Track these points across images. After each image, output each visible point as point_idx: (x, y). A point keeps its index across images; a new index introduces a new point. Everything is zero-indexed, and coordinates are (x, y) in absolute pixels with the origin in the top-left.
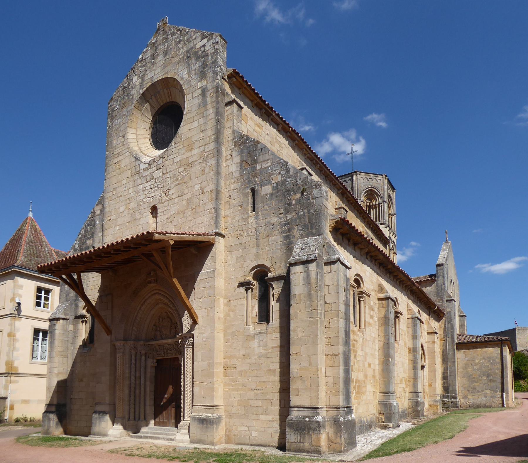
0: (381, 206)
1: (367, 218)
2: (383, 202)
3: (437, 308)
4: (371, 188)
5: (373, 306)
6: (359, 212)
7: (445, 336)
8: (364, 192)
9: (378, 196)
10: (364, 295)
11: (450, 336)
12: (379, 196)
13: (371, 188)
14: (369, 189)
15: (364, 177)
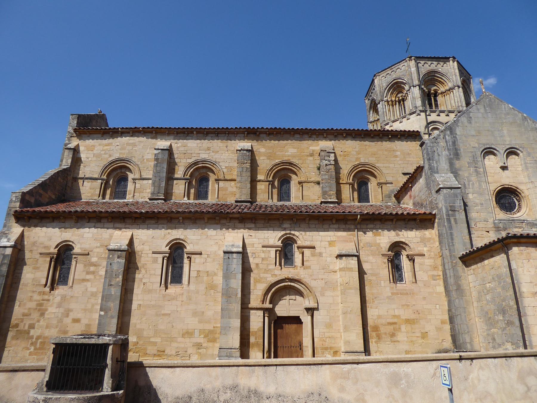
0: (409, 93)
1: (324, 132)
2: (410, 88)
3: (359, 216)
4: (394, 82)
5: (96, 262)
6: (303, 134)
7: (441, 249)
8: (386, 91)
9: (405, 84)
10: (74, 256)
11: (447, 248)
12: (406, 83)
13: (394, 82)
14: (393, 83)
15: (384, 75)
